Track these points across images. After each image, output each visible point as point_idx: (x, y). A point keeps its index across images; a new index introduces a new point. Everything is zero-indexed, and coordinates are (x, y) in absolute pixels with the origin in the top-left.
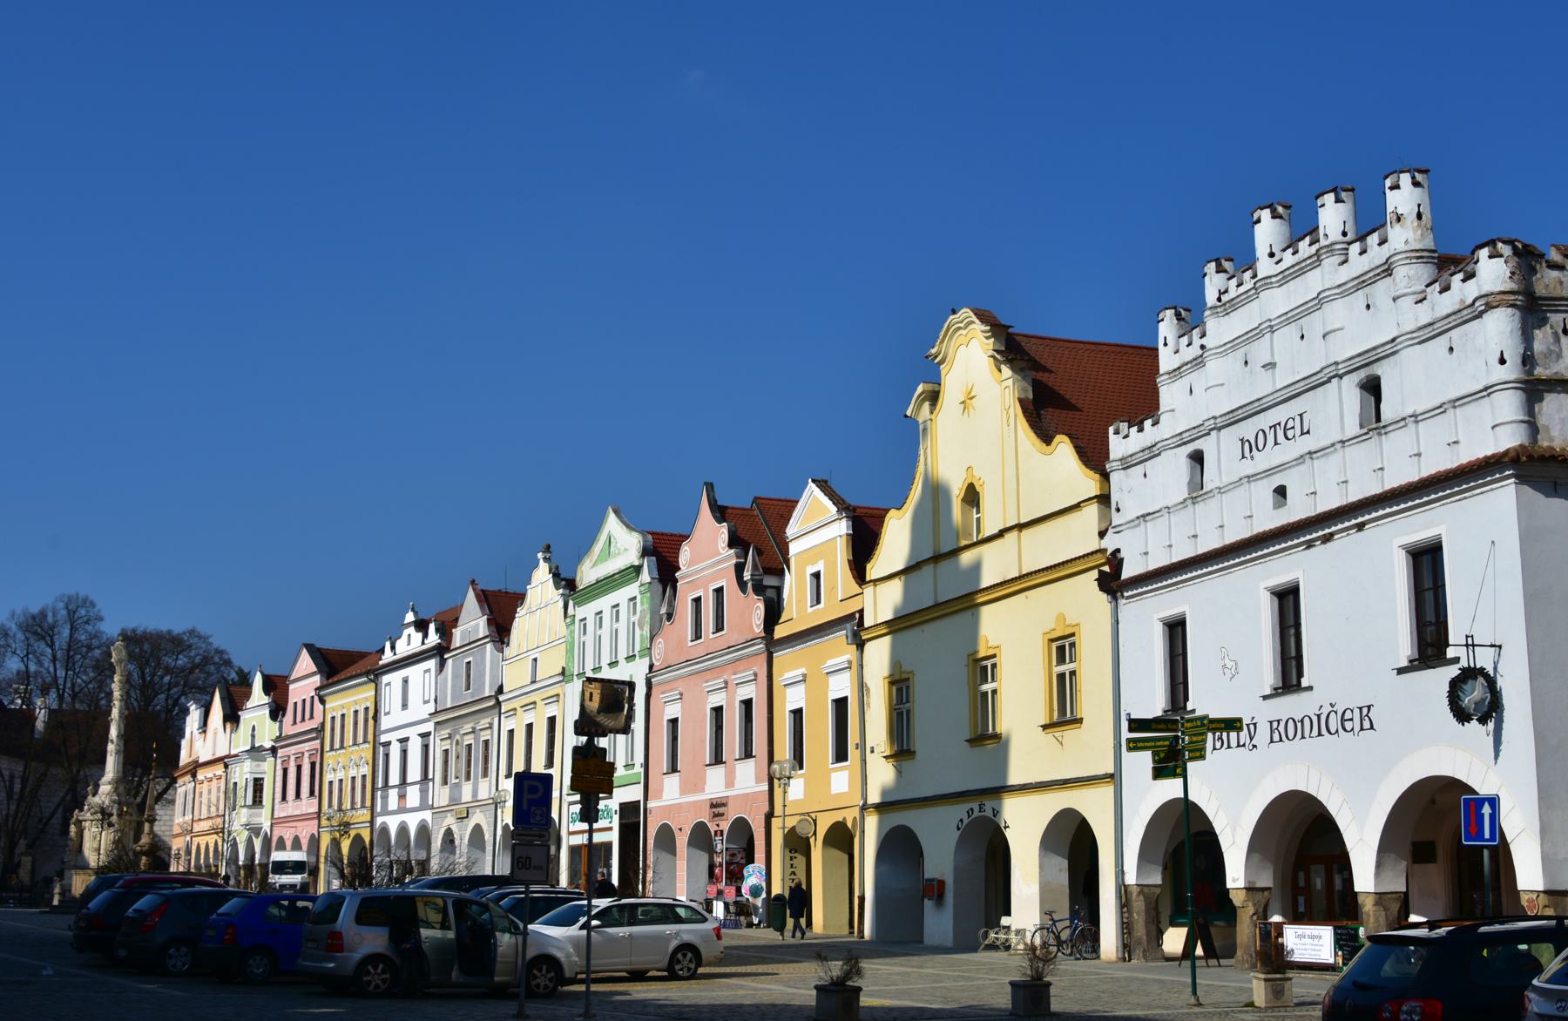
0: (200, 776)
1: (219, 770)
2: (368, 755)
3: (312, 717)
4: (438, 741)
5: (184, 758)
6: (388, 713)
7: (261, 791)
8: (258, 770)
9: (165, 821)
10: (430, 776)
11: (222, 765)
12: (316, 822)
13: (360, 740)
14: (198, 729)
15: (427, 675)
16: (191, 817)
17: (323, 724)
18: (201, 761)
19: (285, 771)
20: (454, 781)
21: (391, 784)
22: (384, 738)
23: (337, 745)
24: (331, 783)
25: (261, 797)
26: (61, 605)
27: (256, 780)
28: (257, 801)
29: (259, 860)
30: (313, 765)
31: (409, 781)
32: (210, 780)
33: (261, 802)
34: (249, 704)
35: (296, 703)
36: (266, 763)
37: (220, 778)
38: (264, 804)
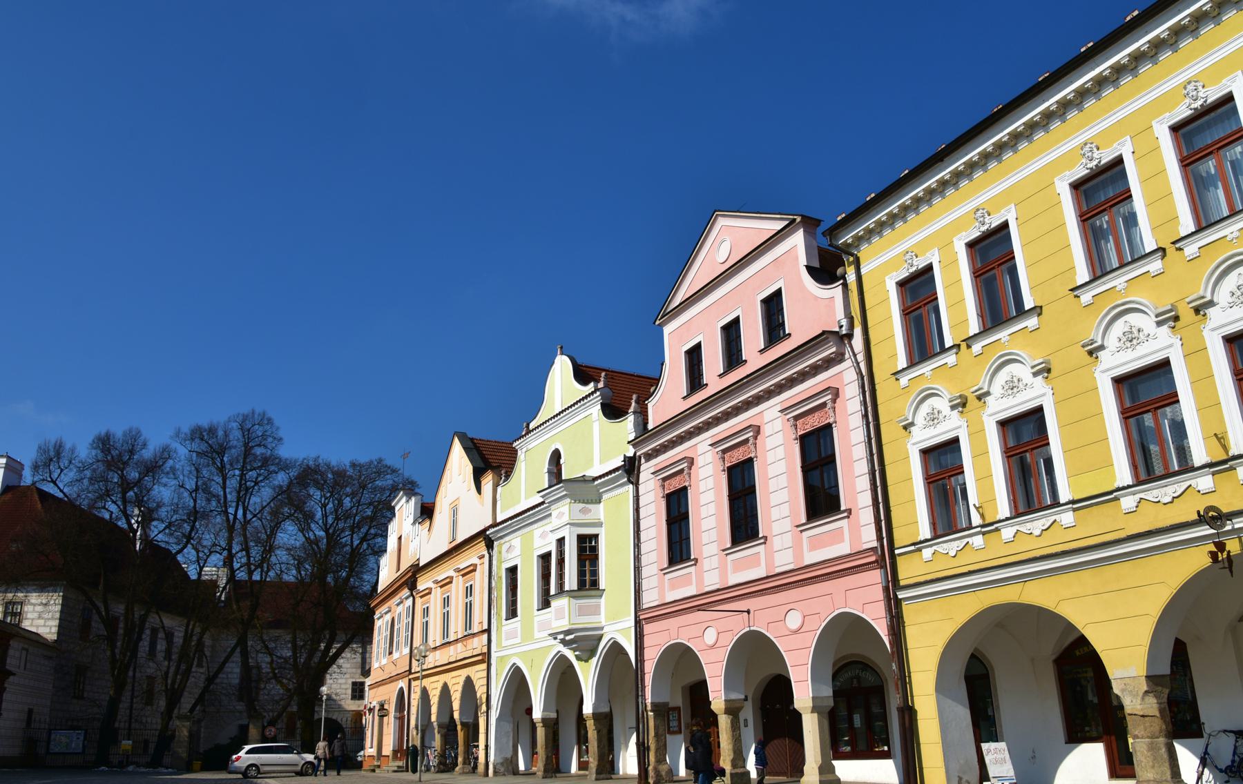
0: (422, 585)
7: (594, 559)
8: (589, 518)
9: (341, 684)
11: (483, 544)
12: (875, 577)
14: (414, 523)
16: (406, 651)
18: (421, 565)
25: (595, 573)
26: (235, 425)
27: (582, 539)
28: (589, 582)
29: (595, 706)
32: (448, 580)
33: (595, 584)
36: (602, 503)
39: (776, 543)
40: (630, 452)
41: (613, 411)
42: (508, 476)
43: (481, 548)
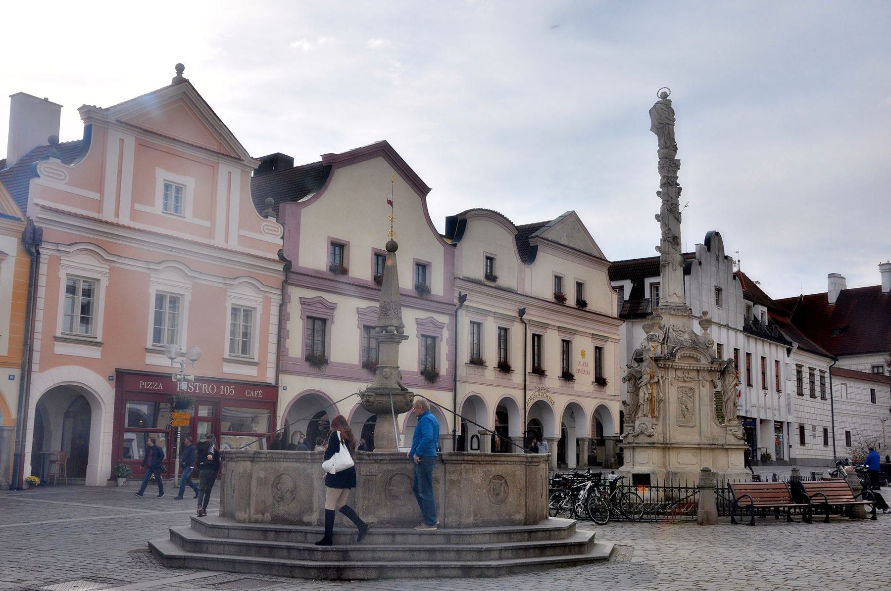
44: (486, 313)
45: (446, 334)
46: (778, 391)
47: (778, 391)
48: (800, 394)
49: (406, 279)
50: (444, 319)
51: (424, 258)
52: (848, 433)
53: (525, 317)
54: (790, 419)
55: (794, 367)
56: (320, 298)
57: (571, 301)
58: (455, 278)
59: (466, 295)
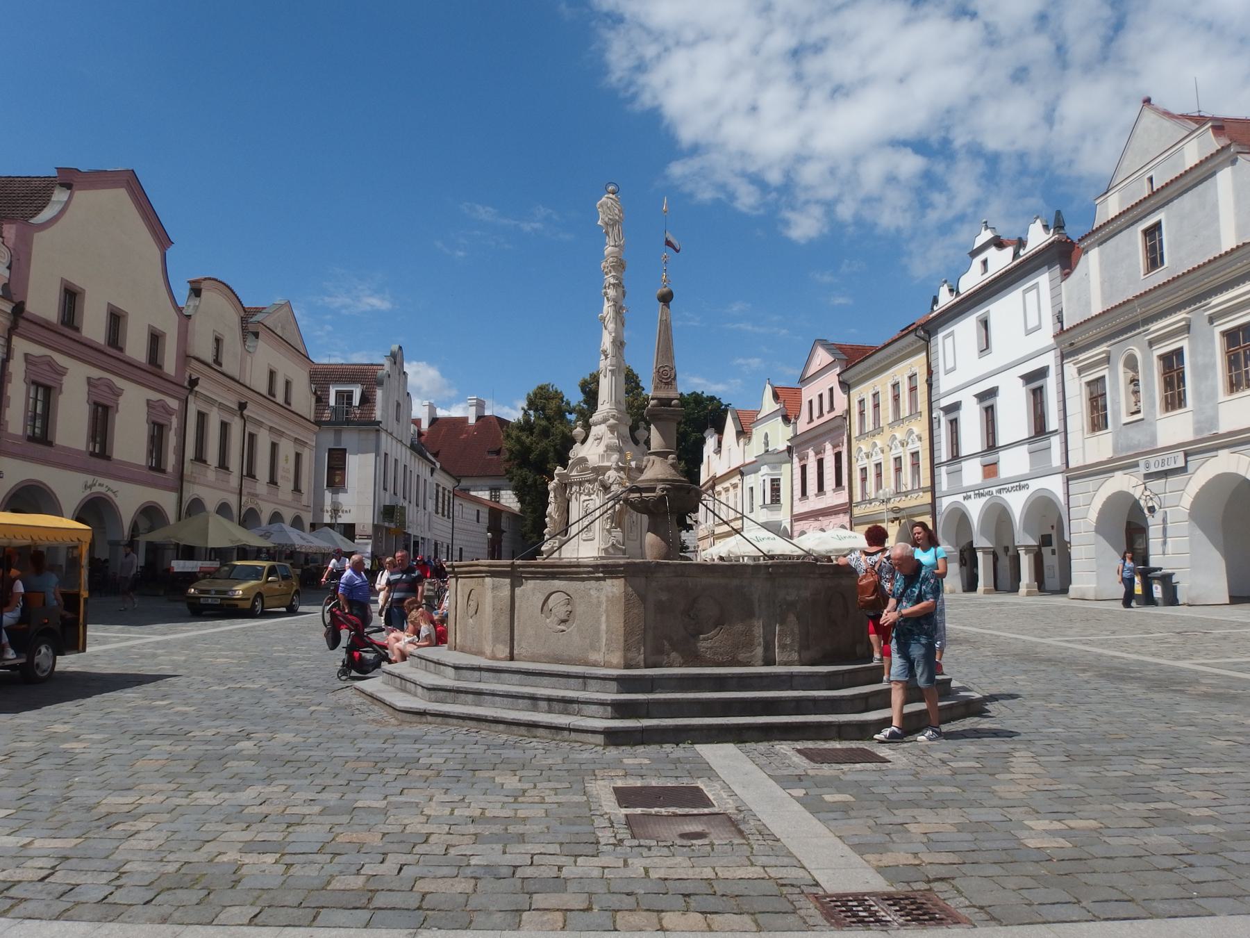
1: (736, 480)
2: (919, 427)
3: (832, 408)
4: (1070, 369)
5: (704, 478)
6: (953, 369)
10: (1053, 423)
13: (905, 410)
15: (1032, 296)
17: (848, 411)
19: (804, 468)
20: (1126, 419)
21: (964, 452)
22: (945, 402)
23: (869, 426)
24: (864, 470)
27: (773, 480)
28: (776, 499)
30: (838, 457)
31: (1001, 442)
32: (727, 490)
34: (759, 416)
35: (811, 402)
37: (735, 486)
38: (782, 502)
39: (827, 493)
40: (789, 444)
41: (786, 419)
42: (750, 439)
43: (739, 477)
44: (210, 401)
45: (175, 421)
46: (425, 509)
47: (425, 509)
48: (437, 512)
49: (136, 348)
50: (174, 404)
51: (160, 326)
52: (461, 549)
53: (246, 412)
54: (428, 535)
55: (435, 486)
56: (49, 359)
57: (280, 399)
58: (188, 356)
59: (198, 378)
